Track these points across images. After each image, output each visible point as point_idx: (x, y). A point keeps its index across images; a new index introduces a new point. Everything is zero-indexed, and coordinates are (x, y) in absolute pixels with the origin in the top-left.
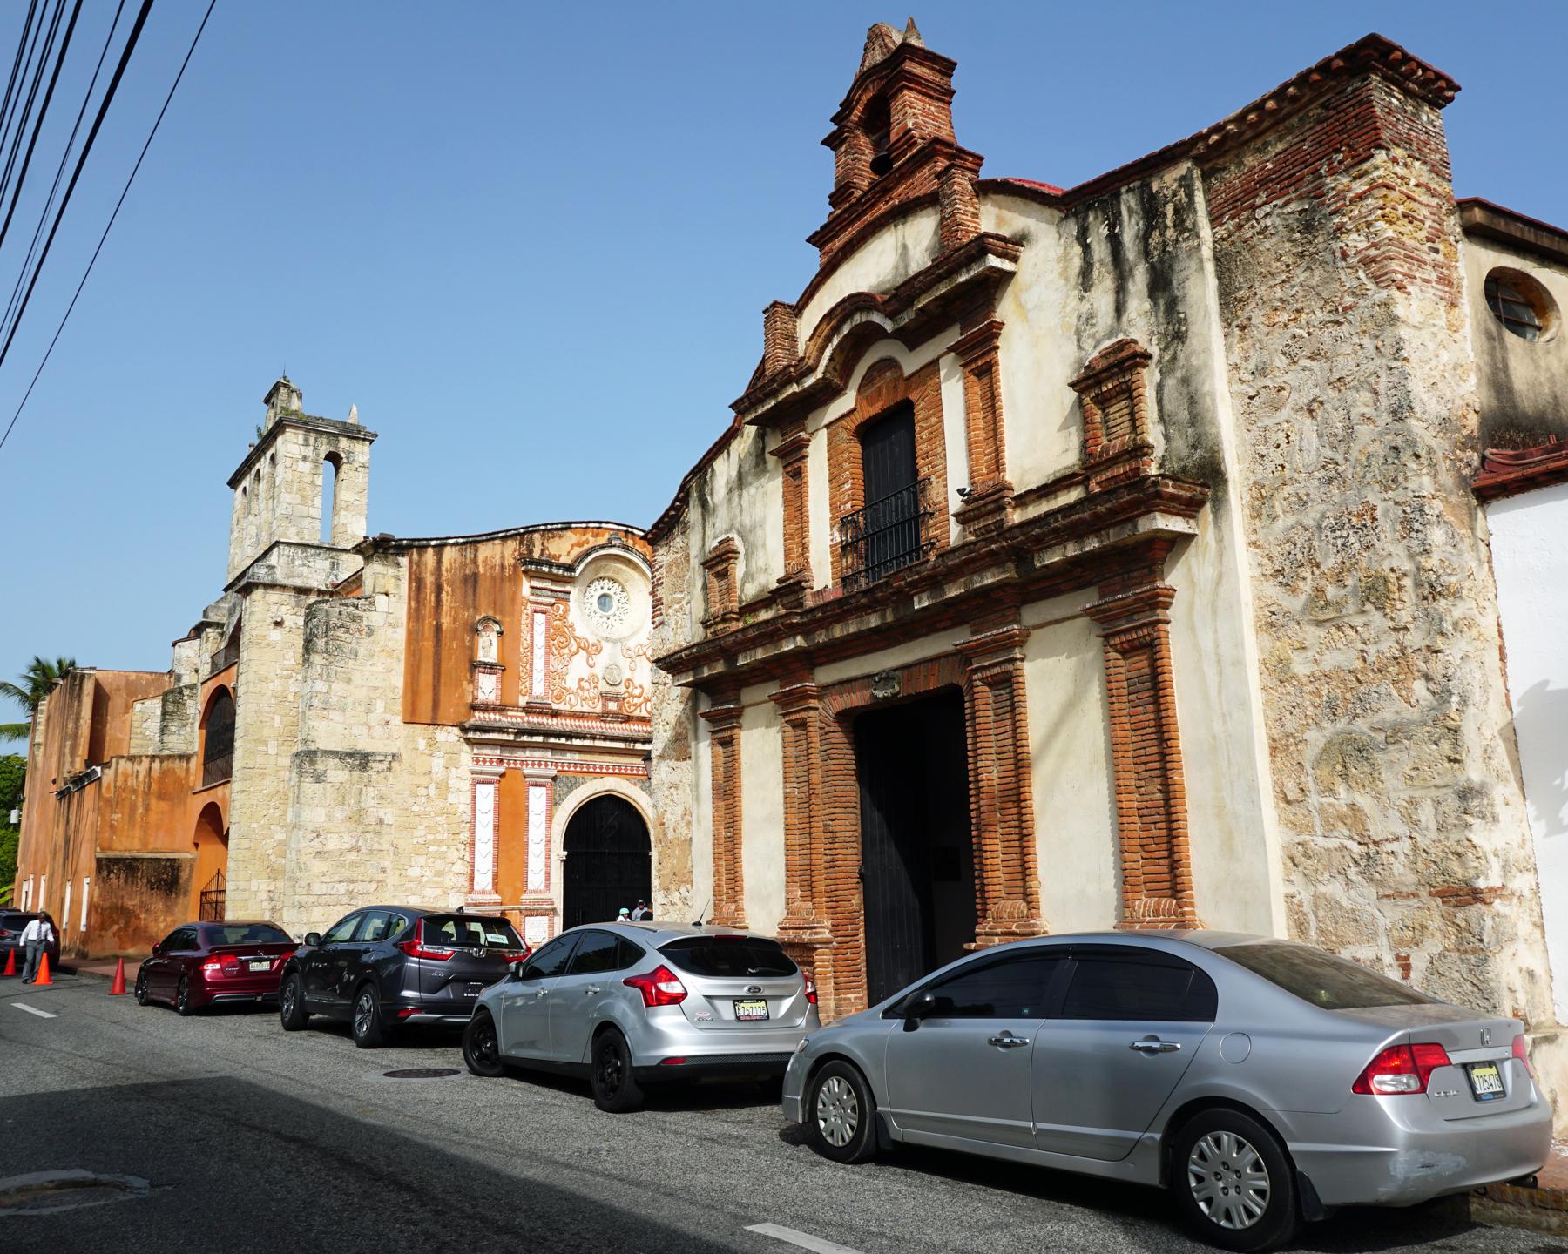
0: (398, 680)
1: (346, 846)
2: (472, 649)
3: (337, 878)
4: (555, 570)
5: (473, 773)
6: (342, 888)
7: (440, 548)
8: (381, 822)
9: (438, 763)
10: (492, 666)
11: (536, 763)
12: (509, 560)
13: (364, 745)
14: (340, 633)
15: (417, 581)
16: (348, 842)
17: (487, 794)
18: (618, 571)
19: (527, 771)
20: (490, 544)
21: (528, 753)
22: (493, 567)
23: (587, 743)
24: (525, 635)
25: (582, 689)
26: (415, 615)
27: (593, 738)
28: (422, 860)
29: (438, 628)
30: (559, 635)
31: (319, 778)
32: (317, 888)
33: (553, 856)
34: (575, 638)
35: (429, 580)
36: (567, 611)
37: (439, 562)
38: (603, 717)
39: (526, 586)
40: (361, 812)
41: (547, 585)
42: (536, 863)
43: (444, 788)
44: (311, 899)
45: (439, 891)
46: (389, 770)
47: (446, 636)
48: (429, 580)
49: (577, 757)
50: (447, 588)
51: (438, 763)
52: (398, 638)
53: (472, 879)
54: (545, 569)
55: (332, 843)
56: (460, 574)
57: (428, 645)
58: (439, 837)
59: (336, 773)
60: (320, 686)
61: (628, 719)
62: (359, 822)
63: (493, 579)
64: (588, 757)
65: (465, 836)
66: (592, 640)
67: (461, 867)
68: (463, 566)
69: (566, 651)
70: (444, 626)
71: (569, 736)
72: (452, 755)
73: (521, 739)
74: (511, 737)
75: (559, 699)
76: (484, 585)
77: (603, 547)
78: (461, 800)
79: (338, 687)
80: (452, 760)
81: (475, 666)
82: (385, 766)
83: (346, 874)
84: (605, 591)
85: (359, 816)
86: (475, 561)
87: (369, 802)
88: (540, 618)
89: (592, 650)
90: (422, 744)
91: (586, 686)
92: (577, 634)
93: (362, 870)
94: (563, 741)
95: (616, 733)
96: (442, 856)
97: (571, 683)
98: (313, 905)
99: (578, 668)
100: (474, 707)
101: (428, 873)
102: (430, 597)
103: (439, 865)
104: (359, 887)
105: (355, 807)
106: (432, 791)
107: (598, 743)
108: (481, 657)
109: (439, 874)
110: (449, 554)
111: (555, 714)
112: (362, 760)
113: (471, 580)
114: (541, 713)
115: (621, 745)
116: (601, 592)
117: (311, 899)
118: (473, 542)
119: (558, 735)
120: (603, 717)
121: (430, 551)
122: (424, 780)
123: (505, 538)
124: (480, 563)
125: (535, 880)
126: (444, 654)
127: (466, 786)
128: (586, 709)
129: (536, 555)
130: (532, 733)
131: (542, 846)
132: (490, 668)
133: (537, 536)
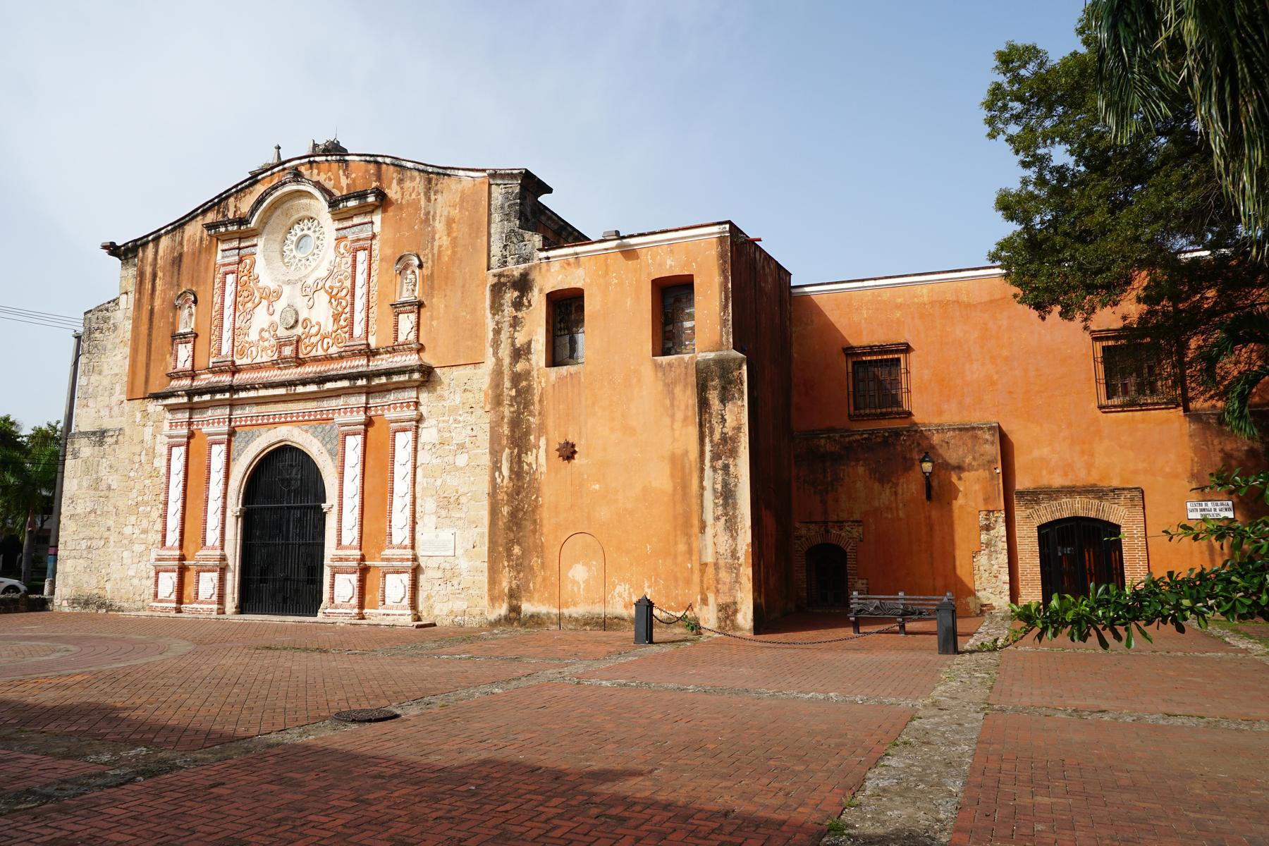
1: (88, 510)
2: (174, 325)
3: (81, 536)
4: (230, 228)
5: (170, 437)
6: (84, 544)
8: (109, 488)
9: (148, 431)
10: (184, 335)
11: (212, 423)
13: (107, 424)
14: (97, 335)
15: (141, 274)
16: (90, 506)
18: (307, 208)
19: (205, 429)
20: (193, 223)
21: (210, 412)
22: (194, 243)
23: (252, 394)
24: (217, 299)
25: (262, 338)
26: (138, 304)
27: (253, 388)
28: (133, 519)
29: (152, 312)
32: (71, 545)
33: (229, 513)
34: (259, 289)
35: (148, 270)
36: (253, 264)
37: (156, 252)
38: (274, 364)
40: (98, 480)
41: (235, 244)
42: (213, 520)
43: (152, 453)
44: (67, 553)
45: (143, 547)
46: (117, 442)
47: (156, 316)
48: (148, 270)
49: (255, 410)
50: (160, 274)
51: (148, 431)
52: (128, 325)
53: (164, 536)
54: (222, 229)
55: (80, 510)
56: (169, 261)
57: (144, 329)
58: (146, 498)
61: (300, 362)
62: (96, 489)
63: (194, 254)
64: (263, 409)
65: (162, 498)
66: (273, 286)
67: (159, 526)
68: (173, 249)
69: (250, 305)
70: (156, 309)
71: (232, 389)
72: (158, 422)
73: (194, 401)
74: (185, 400)
75: (242, 354)
76: (186, 261)
77: (275, 188)
78: (161, 463)
79: (94, 378)
81: (176, 338)
82: (114, 439)
83: (88, 533)
84: (306, 232)
85: (96, 484)
86: (181, 243)
87: (103, 472)
89: (272, 296)
90: (138, 415)
91: (266, 335)
92: (260, 285)
93: (96, 529)
94: (227, 395)
95: (277, 379)
96: (147, 515)
97: (253, 336)
98: (68, 558)
99: (261, 318)
100: (172, 377)
101: (137, 531)
102: (148, 286)
103: (145, 524)
104: (94, 543)
105: (94, 476)
106: (143, 458)
107: (263, 393)
108: (182, 330)
109: (145, 532)
110: (165, 242)
111: (235, 370)
113: (177, 261)
114: (222, 372)
115: (282, 391)
116: (300, 233)
117: (67, 553)
118: (179, 225)
119: (222, 390)
120: (274, 364)
121: (151, 245)
122: (137, 449)
123: (204, 212)
124: (185, 243)
125: (212, 537)
126: (154, 336)
127: (165, 452)
128: (264, 360)
129: (231, 216)
130: (201, 392)
131: (220, 503)
133: (232, 200)
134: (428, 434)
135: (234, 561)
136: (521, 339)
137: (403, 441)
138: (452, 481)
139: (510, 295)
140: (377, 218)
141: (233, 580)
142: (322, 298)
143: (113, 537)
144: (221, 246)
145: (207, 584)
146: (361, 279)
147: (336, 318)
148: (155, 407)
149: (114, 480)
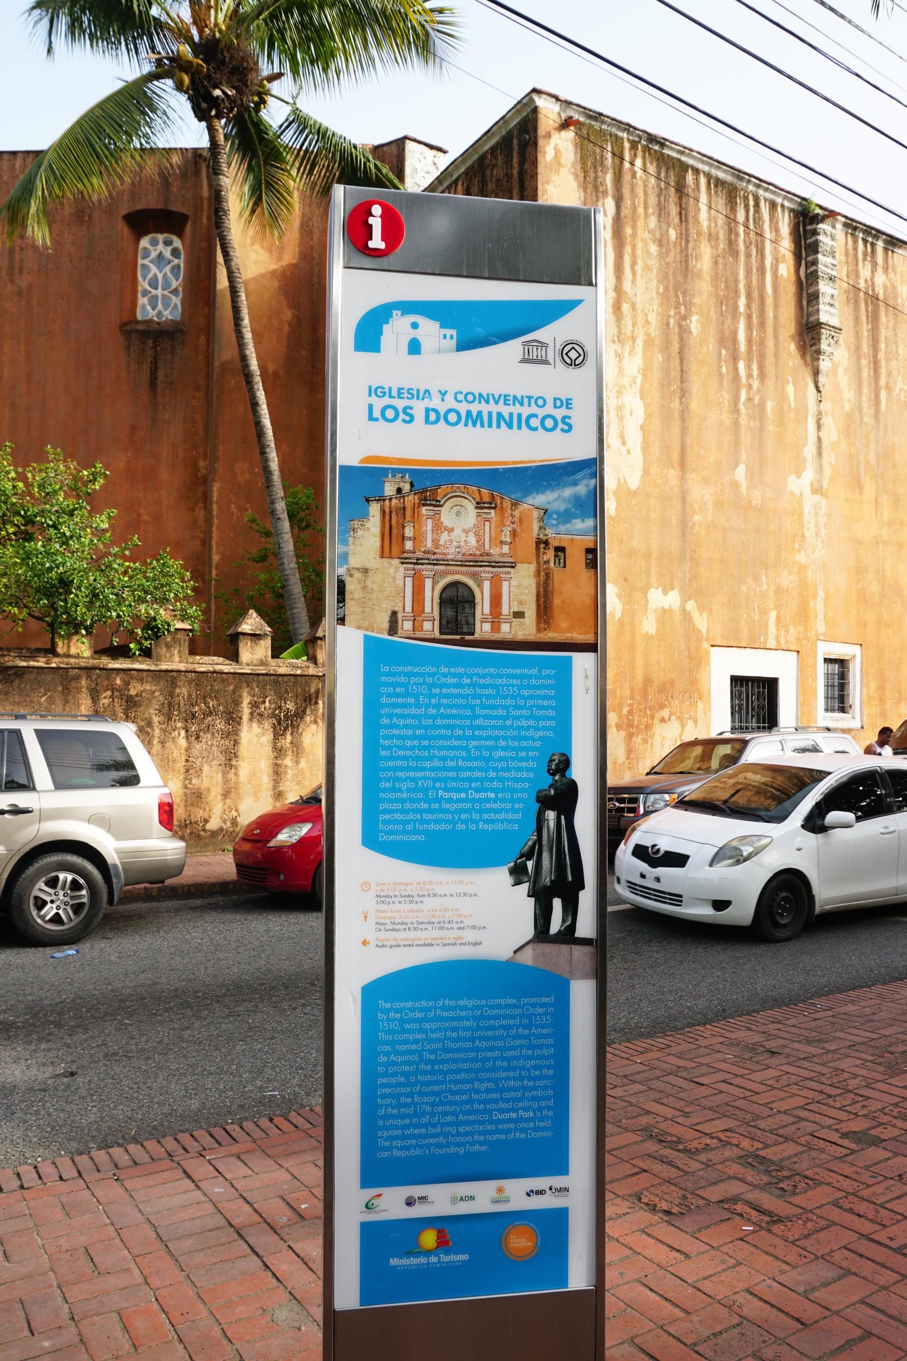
0: (378, 544)
7: (391, 499)
11: (427, 570)
12: (417, 501)
13: (367, 565)
15: (383, 512)
17: (409, 582)
30: (438, 527)
31: (351, 576)
35: (387, 510)
39: (424, 510)
43: (394, 579)
48: (387, 510)
49: (443, 567)
51: (392, 571)
59: (357, 575)
60: (352, 547)
75: (437, 548)
78: (400, 582)
80: (397, 570)
85: (364, 588)
87: (369, 583)
88: (429, 521)
99: (444, 537)
110: (394, 501)
112: (366, 571)
125: (428, 609)
132: (410, 539)
134: (514, 583)
135: (437, 617)
136: (545, 558)
137: (505, 585)
138: (523, 597)
139: (542, 546)
140: (493, 511)
141: (437, 623)
142: (471, 534)
143: (376, 608)
144: (424, 508)
145: (427, 626)
146: (487, 531)
147: (478, 541)
148: (396, 562)
149: (375, 587)
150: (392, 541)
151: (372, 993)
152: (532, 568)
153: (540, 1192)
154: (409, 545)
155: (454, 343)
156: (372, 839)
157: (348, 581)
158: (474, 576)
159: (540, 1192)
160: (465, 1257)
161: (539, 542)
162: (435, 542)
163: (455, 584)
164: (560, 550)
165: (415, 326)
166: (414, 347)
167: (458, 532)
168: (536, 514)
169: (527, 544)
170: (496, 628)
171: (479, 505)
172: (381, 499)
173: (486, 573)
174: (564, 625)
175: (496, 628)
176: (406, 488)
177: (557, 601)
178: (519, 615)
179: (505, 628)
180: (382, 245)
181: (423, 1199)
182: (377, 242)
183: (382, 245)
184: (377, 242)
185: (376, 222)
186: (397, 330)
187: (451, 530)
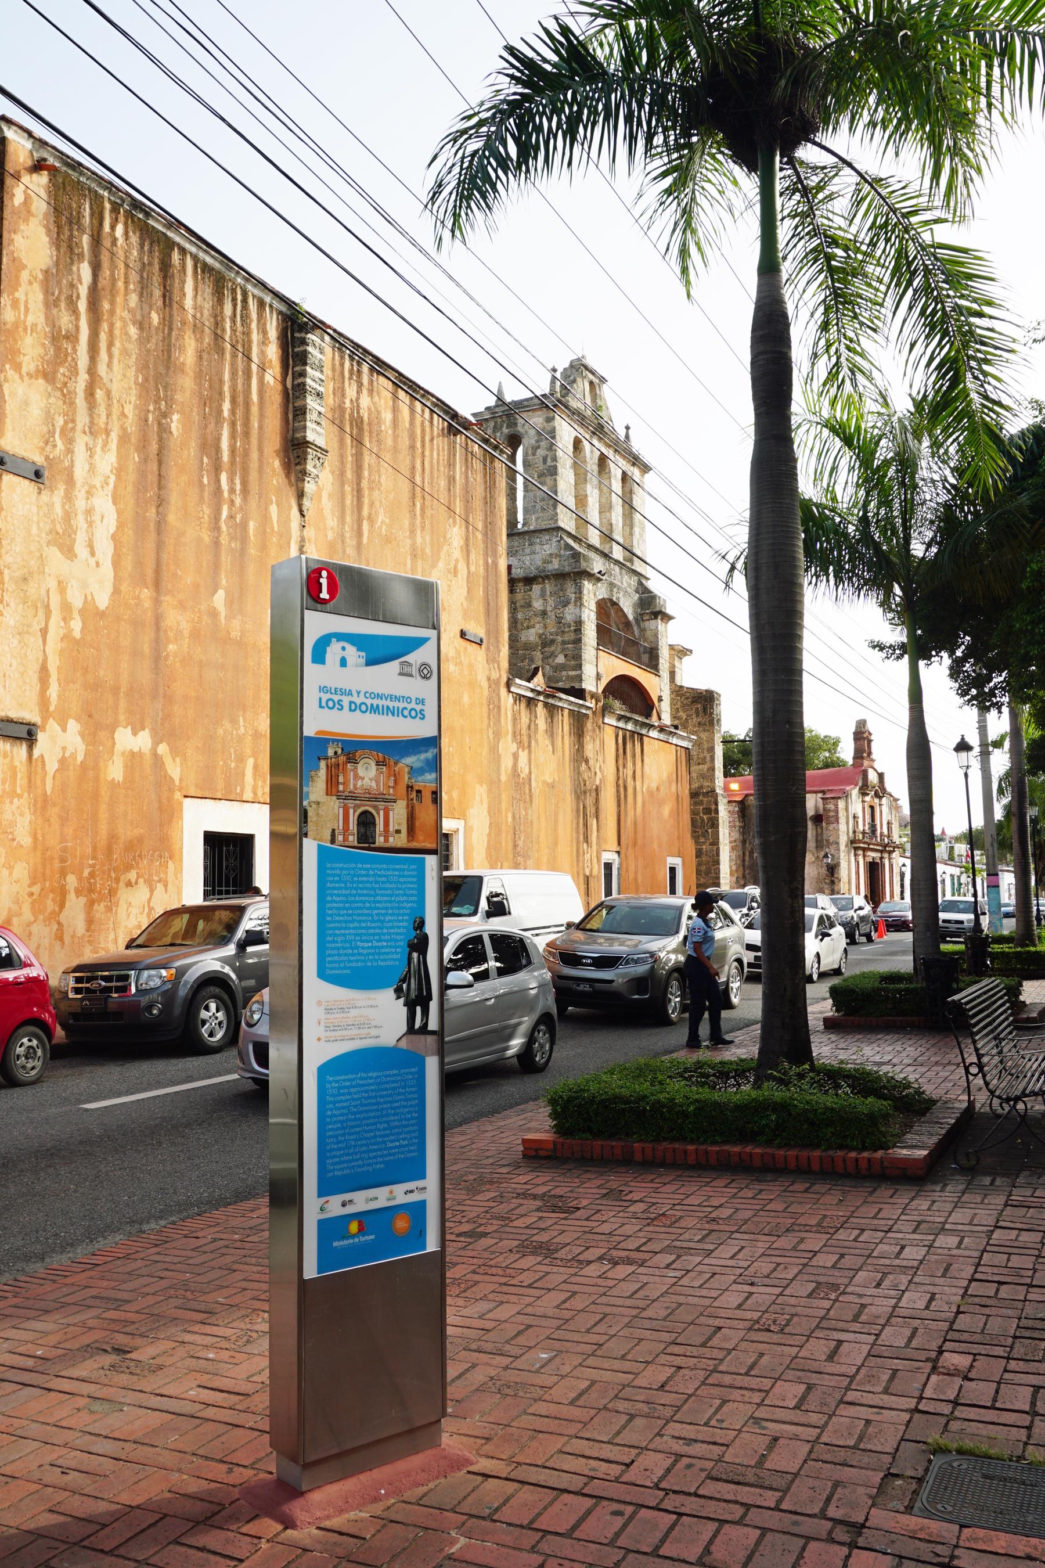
11: (351, 803)
30: (357, 777)
145: (351, 838)
150: (332, 785)
151: (324, 1071)
152: (405, 803)
153: (412, 1192)
154: (341, 788)
155: (363, 661)
156: (323, 974)
157: (309, 810)
158: (376, 807)
159: (412, 1192)
160: (373, 1237)
161: (408, 787)
162: (355, 785)
163: (365, 812)
164: (419, 792)
165: (344, 649)
166: (343, 662)
167: (366, 780)
168: (407, 770)
169: (402, 789)
170: (386, 841)
171: (378, 764)
172: (326, 758)
173: (381, 805)
174: (421, 838)
175: (386, 841)
176: (340, 751)
177: (417, 824)
178: (398, 832)
179: (391, 839)
180: (327, 597)
181: (351, 1201)
182: (324, 595)
183: (327, 597)
184: (324, 595)
185: (324, 581)
186: (334, 650)
187: (363, 779)
